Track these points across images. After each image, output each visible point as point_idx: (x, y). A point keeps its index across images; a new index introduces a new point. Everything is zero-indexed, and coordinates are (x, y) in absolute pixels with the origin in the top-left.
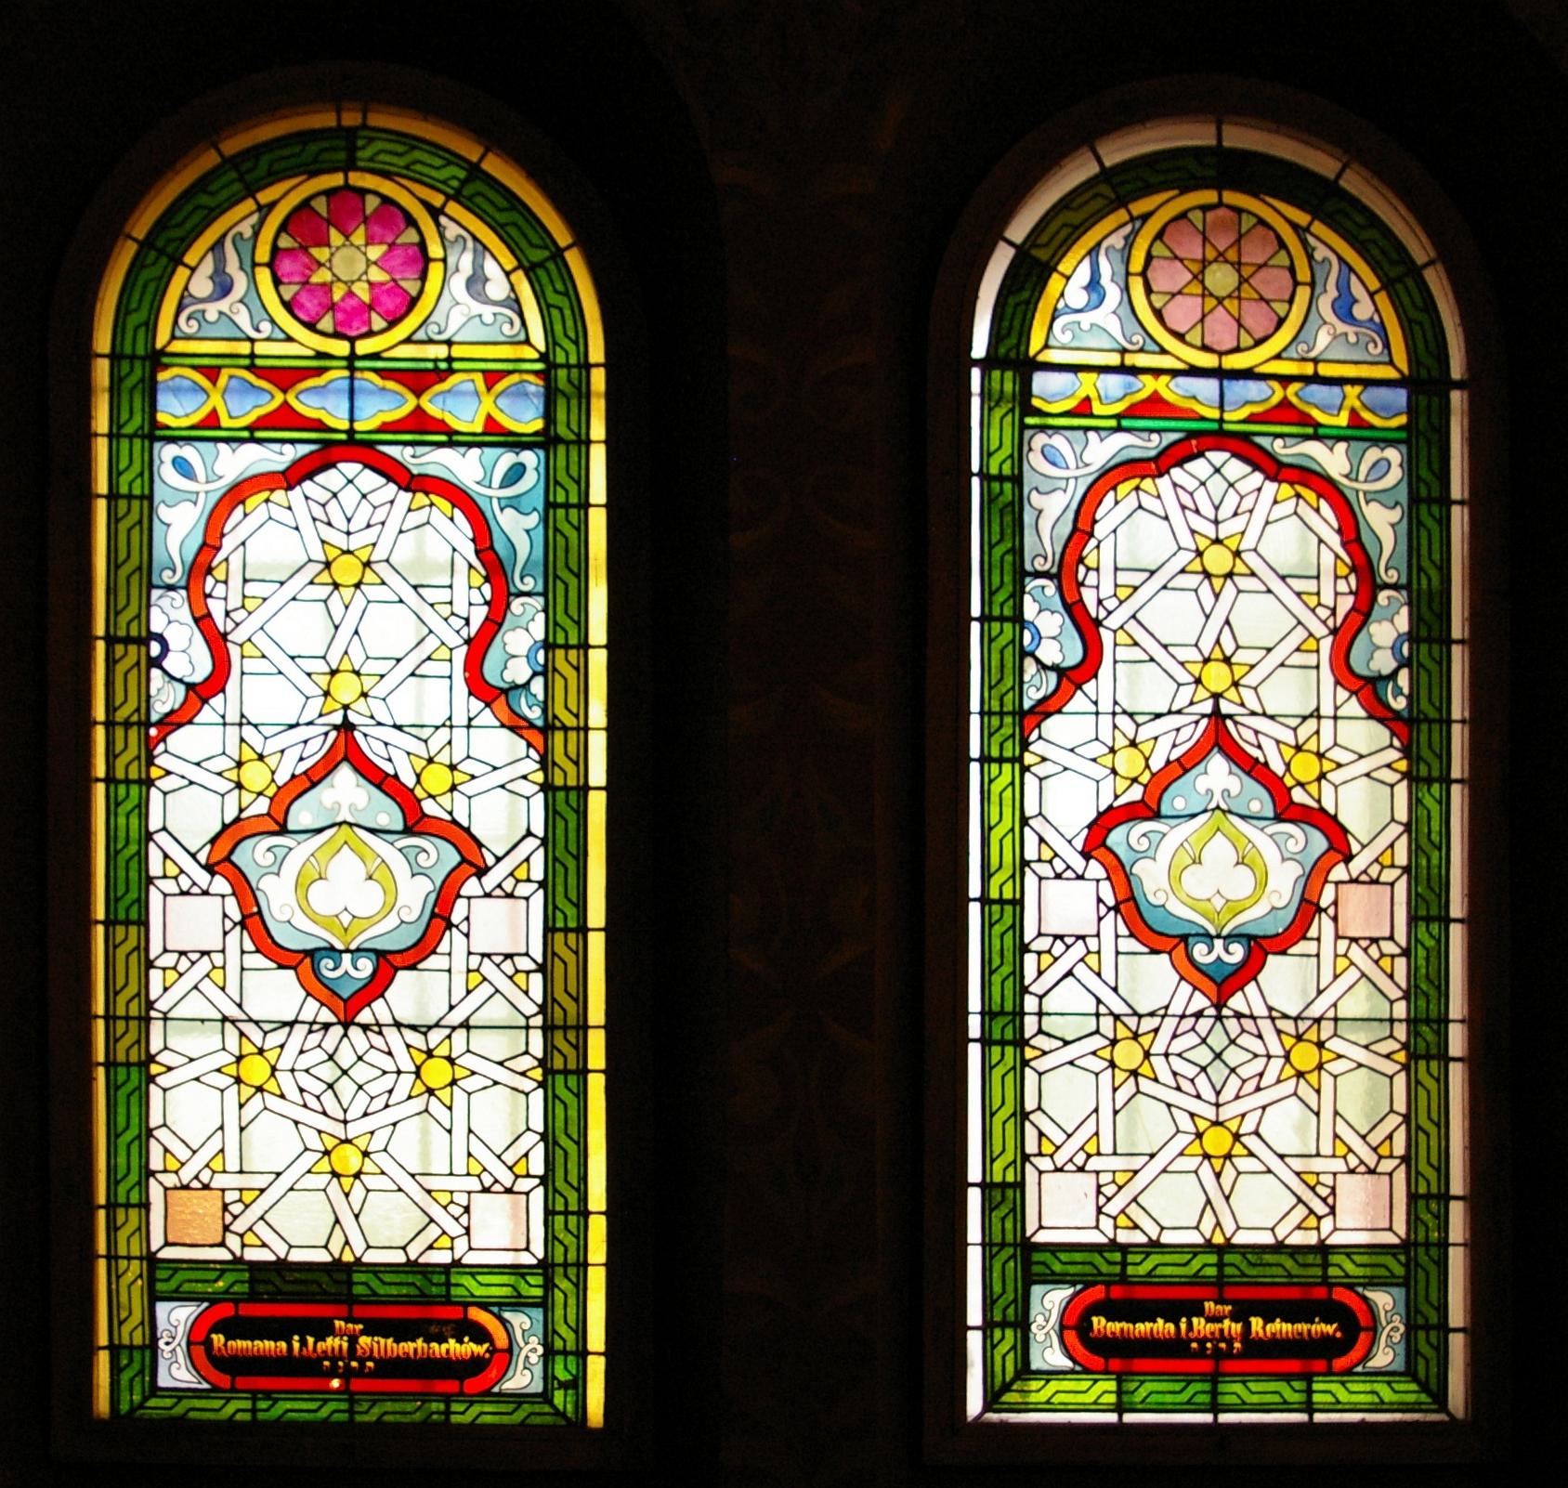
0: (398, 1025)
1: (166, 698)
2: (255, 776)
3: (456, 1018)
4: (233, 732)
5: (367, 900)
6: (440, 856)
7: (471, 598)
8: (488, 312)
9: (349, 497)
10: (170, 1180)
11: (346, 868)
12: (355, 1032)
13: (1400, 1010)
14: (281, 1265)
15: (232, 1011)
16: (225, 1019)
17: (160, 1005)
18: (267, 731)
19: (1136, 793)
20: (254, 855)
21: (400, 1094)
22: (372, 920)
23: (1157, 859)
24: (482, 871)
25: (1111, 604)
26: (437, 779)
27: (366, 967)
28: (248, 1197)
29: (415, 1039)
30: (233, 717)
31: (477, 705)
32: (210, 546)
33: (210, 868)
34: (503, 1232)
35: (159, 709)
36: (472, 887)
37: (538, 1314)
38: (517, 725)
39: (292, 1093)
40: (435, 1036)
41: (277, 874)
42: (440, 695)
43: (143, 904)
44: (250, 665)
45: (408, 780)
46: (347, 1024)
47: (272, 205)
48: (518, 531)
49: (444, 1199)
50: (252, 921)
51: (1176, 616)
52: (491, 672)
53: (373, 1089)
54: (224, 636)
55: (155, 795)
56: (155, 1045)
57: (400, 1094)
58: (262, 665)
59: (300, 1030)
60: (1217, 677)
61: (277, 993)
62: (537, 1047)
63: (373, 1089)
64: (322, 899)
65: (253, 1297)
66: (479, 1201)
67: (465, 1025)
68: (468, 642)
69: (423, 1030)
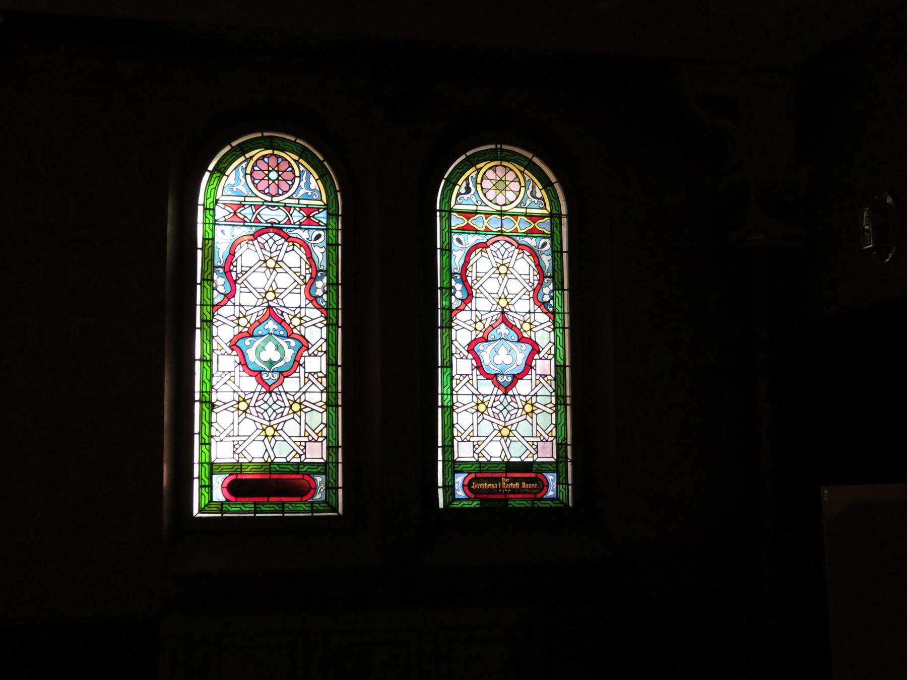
0: (519, 395)
1: (456, 304)
2: (480, 326)
3: (533, 393)
4: (474, 313)
5: (508, 360)
6: (527, 348)
7: (534, 278)
8: (536, 201)
9: (271, 242)
10: (217, 439)
11: (503, 351)
12: (508, 397)
13: (553, 394)
14: (489, 462)
15: (237, 389)
16: (234, 392)
17: (456, 389)
18: (247, 308)
19: (481, 335)
20: (480, 347)
21: (519, 415)
22: (510, 365)
23: (486, 352)
24: (539, 352)
25: (475, 282)
26: (526, 327)
27: (510, 379)
28: (298, 444)
29: (523, 399)
30: (474, 309)
31: (536, 307)
32: (232, 254)
33: (468, 351)
34: (547, 454)
35: (454, 307)
36: (536, 356)
37: (324, 477)
38: (547, 313)
39: (492, 414)
40: (528, 398)
41: (486, 352)
42: (524, 305)
43: (451, 361)
44: (478, 295)
45: (519, 327)
46: (270, 392)
47: (251, 158)
48: (546, 260)
49: (298, 444)
50: (479, 367)
51: (492, 286)
52: (540, 299)
53: (511, 413)
54: (471, 287)
55: (453, 331)
56: (455, 401)
57: (519, 415)
58: (481, 295)
59: (493, 397)
60: (270, 296)
61: (487, 387)
62: (554, 402)
63: (511, 413)
64: (498, 360)
65: (480, 472)
66: (540, 444)
67: (536, 395)
68: (534, 290)
69: (525, 396)
